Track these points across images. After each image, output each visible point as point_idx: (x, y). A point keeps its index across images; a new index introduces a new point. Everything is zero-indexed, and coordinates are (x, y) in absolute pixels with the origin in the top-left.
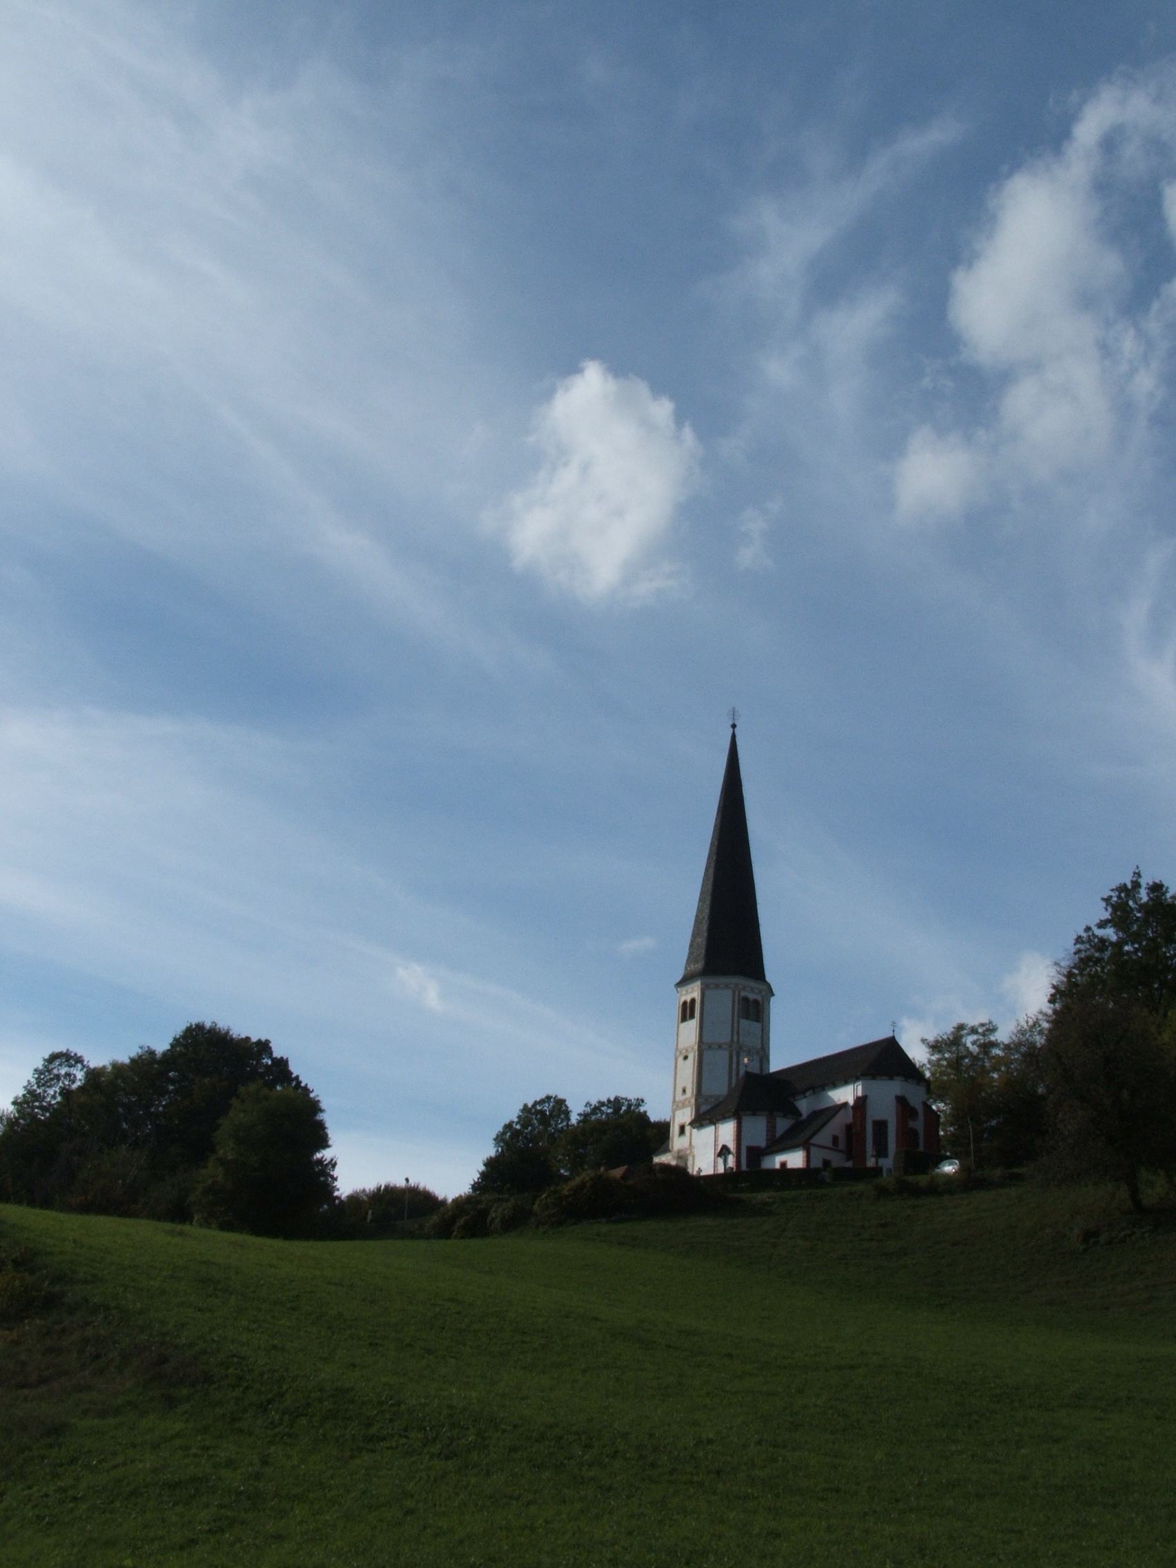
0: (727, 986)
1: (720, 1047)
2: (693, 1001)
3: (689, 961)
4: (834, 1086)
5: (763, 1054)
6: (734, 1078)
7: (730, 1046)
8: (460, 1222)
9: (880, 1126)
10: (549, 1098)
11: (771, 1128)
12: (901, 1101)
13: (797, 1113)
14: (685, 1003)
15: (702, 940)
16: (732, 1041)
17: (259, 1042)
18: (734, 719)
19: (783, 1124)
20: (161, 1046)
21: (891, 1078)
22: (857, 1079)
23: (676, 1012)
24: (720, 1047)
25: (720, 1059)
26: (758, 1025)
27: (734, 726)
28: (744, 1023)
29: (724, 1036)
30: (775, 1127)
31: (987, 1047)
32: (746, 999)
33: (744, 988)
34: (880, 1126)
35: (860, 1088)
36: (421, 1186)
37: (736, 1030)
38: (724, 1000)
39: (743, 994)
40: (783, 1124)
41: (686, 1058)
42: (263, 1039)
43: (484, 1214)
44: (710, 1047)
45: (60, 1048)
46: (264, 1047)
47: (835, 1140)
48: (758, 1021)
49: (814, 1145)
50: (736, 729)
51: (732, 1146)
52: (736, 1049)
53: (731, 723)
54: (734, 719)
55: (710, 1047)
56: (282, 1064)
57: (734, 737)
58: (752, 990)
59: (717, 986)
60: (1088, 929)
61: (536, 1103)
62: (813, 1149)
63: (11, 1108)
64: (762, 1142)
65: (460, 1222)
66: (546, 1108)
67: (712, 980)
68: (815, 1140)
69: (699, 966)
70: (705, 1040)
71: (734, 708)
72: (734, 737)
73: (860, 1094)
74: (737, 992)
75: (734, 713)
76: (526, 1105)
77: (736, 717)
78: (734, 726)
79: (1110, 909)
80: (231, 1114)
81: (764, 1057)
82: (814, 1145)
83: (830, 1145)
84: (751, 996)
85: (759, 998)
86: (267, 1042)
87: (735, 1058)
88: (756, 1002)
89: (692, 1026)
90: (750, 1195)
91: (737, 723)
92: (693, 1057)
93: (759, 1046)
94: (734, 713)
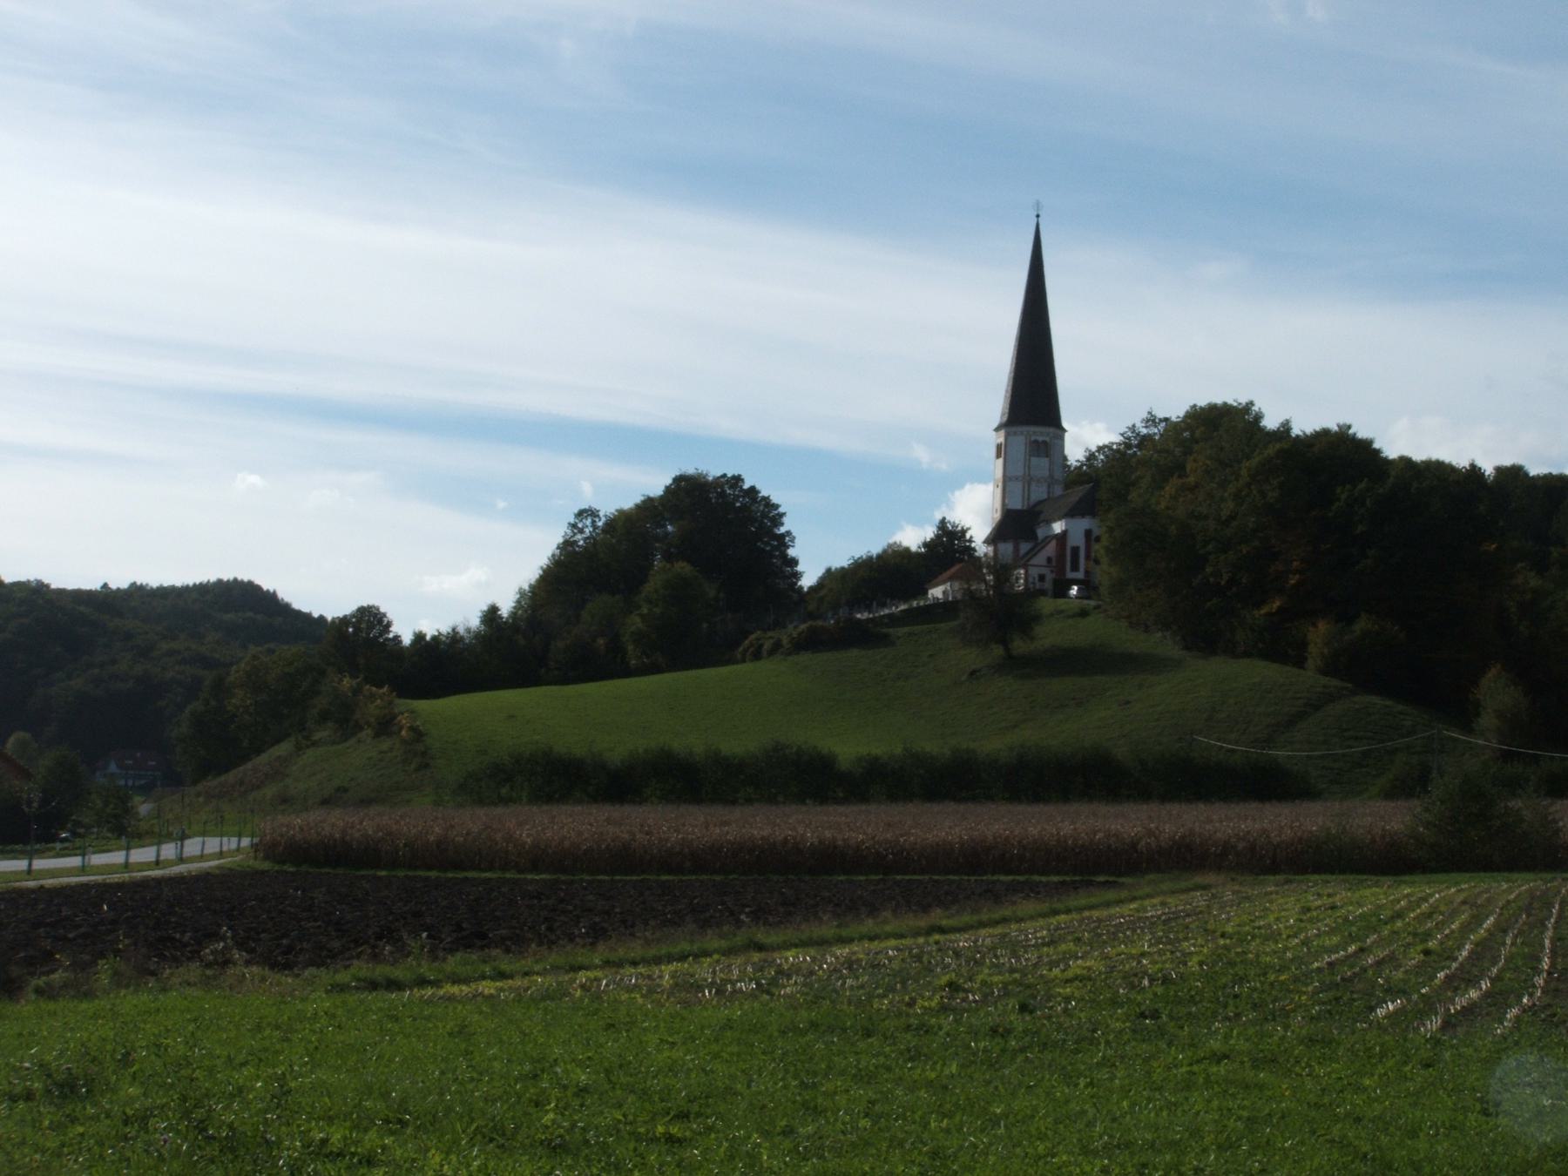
0: (1022, 433)
3: (1003, 414)
6: (1026, 503)
9: (1075, 550)
11: (1016, 549)
12: (1088, 533)
13: (1035, 537)
16: (1025, 474)
18: (1038, 210)
19: (1025, 547)
21: (1083, 517)
22: (1063, 518)
25: (1017, 487)
26: (1046, 460)
27: (1038, 216)
28: (1034, 460)
29: (1019, 471)
31: (987, 558)
34: (1075, 550)
35: (1064, 524)
38: (1020, 443)
39: (1033, 439)
41: (998, 486)
43: (761, 646)
44: (1010, 479)
46: (737, 480)
47: (1049, 560)
48: (1047, 456)
49: (1031, 565)
50: (1040, 219)
53: (1036, 213)
54: (1038, 210)
55: (1010, 479)
68: (1031, 562)
69: (1005, 419)
73: (1064, 528)
75: (1038, 205)
78: (1038, 216)
82: (1031, 565)
83: (1044, 563)
84: (1040, 439)
85: (1047, 439)
86: (739, 476)
88: (1044, 442)
89: (1001, 461)
90: (891, 630)
91: (1040, 213)
92: (1000, 484)
94: (1038, 205)
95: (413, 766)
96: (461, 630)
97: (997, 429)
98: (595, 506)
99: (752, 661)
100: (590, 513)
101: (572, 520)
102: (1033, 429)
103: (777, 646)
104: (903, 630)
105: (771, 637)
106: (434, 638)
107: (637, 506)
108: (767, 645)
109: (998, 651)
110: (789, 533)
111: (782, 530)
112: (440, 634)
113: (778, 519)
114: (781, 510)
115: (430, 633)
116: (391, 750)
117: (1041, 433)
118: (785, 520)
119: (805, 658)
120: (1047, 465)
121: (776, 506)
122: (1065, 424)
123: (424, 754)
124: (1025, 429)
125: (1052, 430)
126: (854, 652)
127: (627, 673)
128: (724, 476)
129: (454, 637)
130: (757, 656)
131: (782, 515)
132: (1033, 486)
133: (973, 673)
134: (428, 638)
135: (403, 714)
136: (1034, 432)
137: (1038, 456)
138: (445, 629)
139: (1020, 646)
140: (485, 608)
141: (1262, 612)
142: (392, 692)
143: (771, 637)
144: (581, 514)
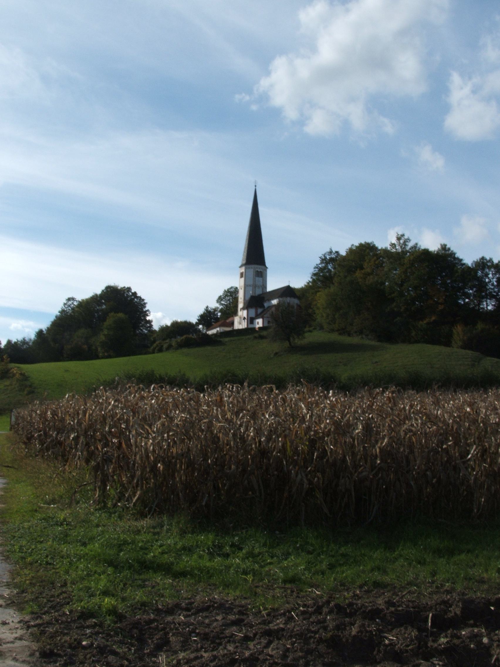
0: (252, 268)
1: (250, 286)
3: (243, 260)
4: (273, 299)
5: (264, 286)
8: (157, 349)
10: (232, 288)
11: (256, 312)
13: (264, 307)
15: (245, 254)
17: (128, 288)
19: (260, 310)
20: (99, 292)
23: (239, 275)
26: (261, 278)
27: (256, 186)
28: (257, 278)
29: (251, 282)
32: (257, 271)
33: (257, 268)
36: (188, 321)
37: (254, 281)
38: (251, 272)
39: (257, 270)
42: (129, 287)
43: (162, 346)
44: (247, 286)
45: (70, 296)
46: (129, 289)
51: (246, 317)
52: (255, 286)
55: (247, 286)
56: (135, 294)
58: (260, 269)
59: (249, 268)
60: (317, 265)
61: (228, 289)
63: (59, 314)
65: (157, 349)
66: (232, 290)
67: (248, 266)
69: (244, 262)
75: (256, 182)
76: (225, 290)
78: (256, 186)
79: (212, 311)
80: (107, 320)
84: (259, 270)
85: (262, 270)
87: (254, 289)
88: (261, 272)
89: (243, 279)
92: (243, 289)
93: (262, 284)
94: (256, 182)
95: (25, 392)
96: (27, 339)
97: (241, 267)
98: (75, 296)
99: (157, 353)
100: (73, 299)
101: (65, 302)
102: (256, 266)
103: (169, 347)
104: (227, 339)
105: (166, 343)
106: (15, 343)
107: (87, 299)
108: (165, 346)
109: (286, 344)
110: (148, 311)
111: (146, 309)
112: (18, 341)
113: (144, 305)
114: (145, 301)
115: (14, 340)
116: (11, 385)
117: (259, 268)
118: (147, 305)
119: (185, 350)
120: (261, 281)
121: (143, 300)
122: (267, 264)
123: (30, 386)
124: (253, 266)
125: (263, 267)
126: (209, 348)
127: (97, 357)
128: (124, 287)
129: (24, 342)
130: (160, 350)
131: (145, 304)
132: (257, 289)
133: (276, 354)
134: (13, 342)
135: (14, 368)
138: (20, 338)
139: (298, 342)
140: (37, 331)
141: (425, 322)
142: (8, 358)
143: (166, 343)
144: (69, 299)
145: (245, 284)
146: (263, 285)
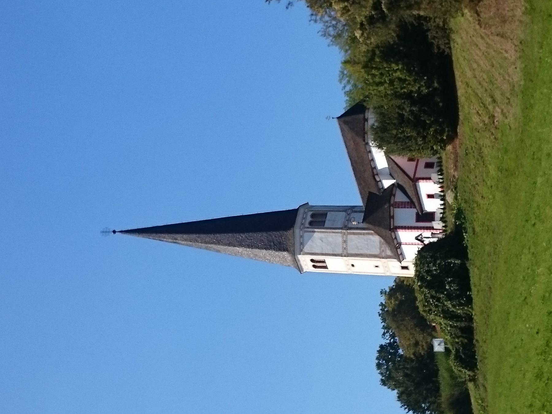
0: (302, 237)
1: (345, 242)
2: (312, 261)
7: (344, 234)
11: (402, 205)
14: (314, 266)
16: (341, 233)
18: (109, 232)
19: (399, 197)
24: (345, 242)
26: (329, 214)
28: (327, 224)
30: (402, 202)
32: (311, 223)
39: (307, 225)
40: (399, 197)
41: (353, 265)
47: (411, 160)
48: (326, 215)
51: (416, 233)
54: (109, 232)
57: (121, 232)
62: (417, 176)
64: (413, 212)
70: (340, 251)
71: (103, 232)
72: (121, 232)
74: (306, 230)
77: (108, 230)
78: (114, 232)
81: (352, 209)
83: (414, 163)
84: (309, 219)
85: (310, 213)
88: (313, 216)
91: (112, 230)
92: (352, 260)
93: (344, 214)
136: (302, 224)
137: (324, 222)
145: (341, 255)
146: (345, 211)
